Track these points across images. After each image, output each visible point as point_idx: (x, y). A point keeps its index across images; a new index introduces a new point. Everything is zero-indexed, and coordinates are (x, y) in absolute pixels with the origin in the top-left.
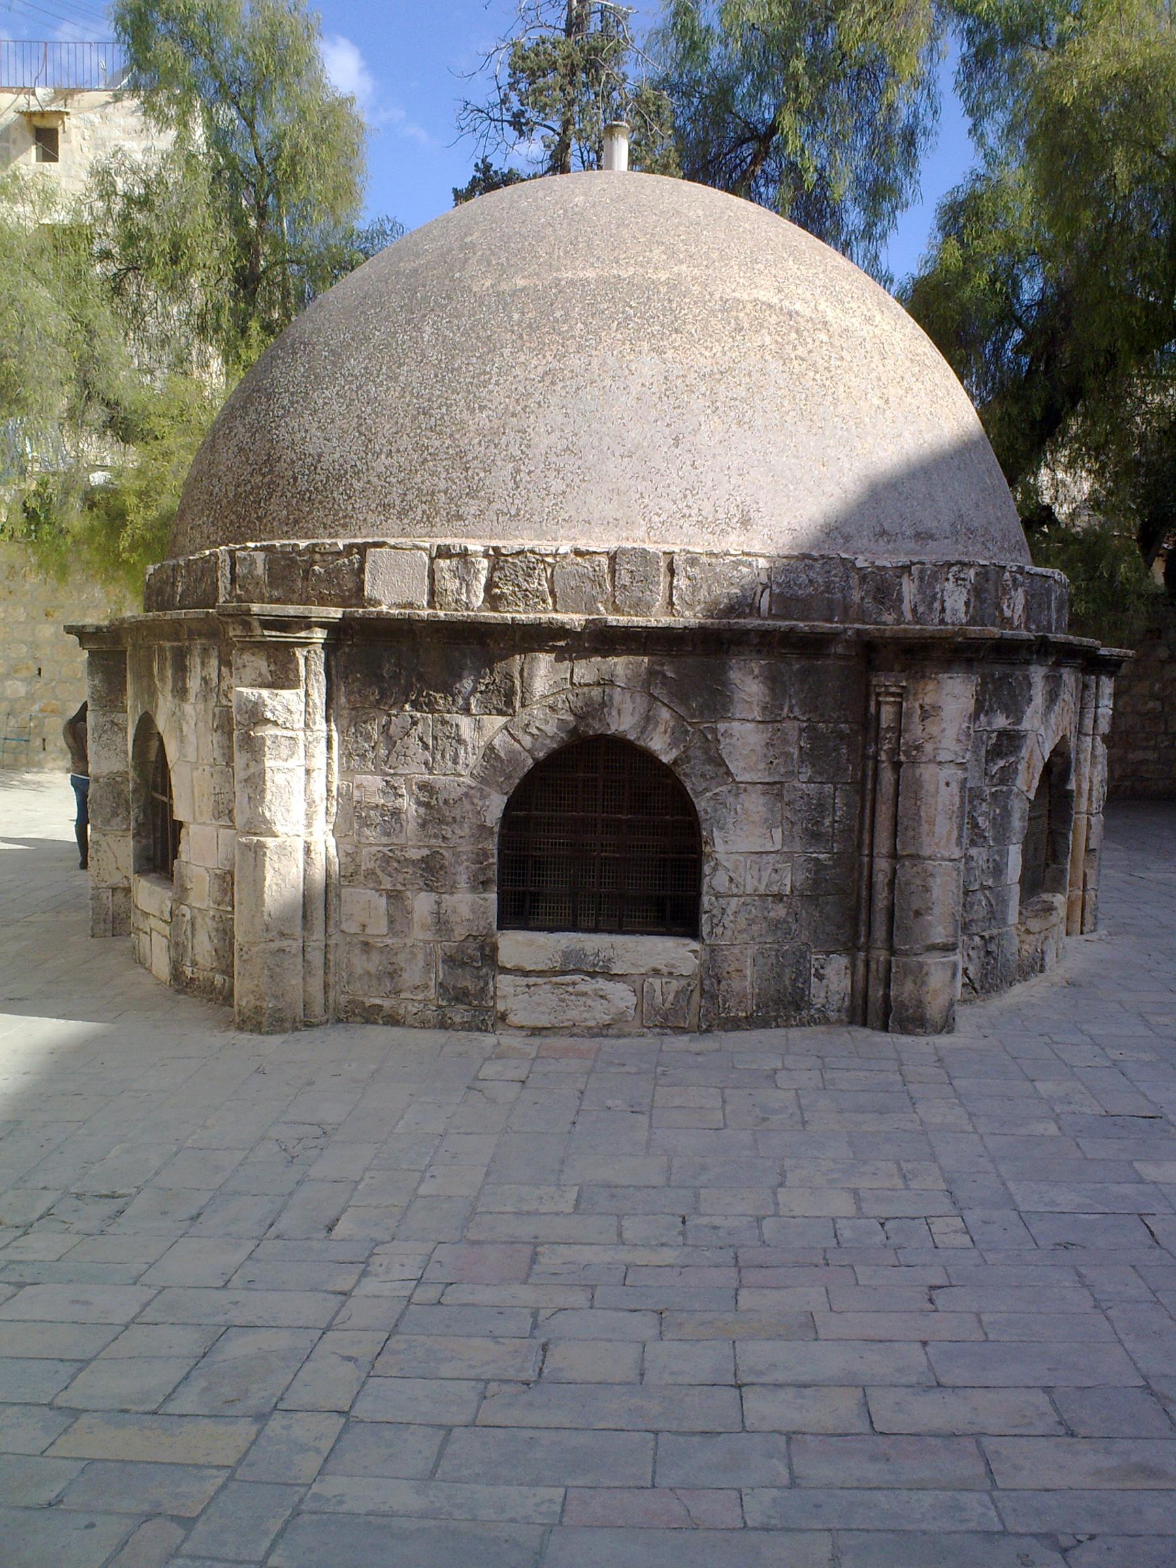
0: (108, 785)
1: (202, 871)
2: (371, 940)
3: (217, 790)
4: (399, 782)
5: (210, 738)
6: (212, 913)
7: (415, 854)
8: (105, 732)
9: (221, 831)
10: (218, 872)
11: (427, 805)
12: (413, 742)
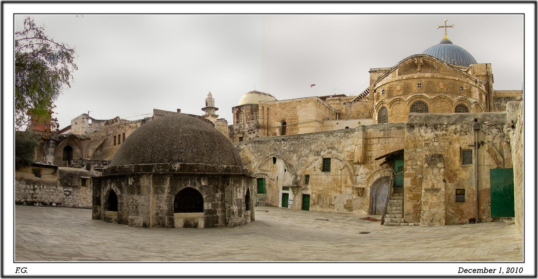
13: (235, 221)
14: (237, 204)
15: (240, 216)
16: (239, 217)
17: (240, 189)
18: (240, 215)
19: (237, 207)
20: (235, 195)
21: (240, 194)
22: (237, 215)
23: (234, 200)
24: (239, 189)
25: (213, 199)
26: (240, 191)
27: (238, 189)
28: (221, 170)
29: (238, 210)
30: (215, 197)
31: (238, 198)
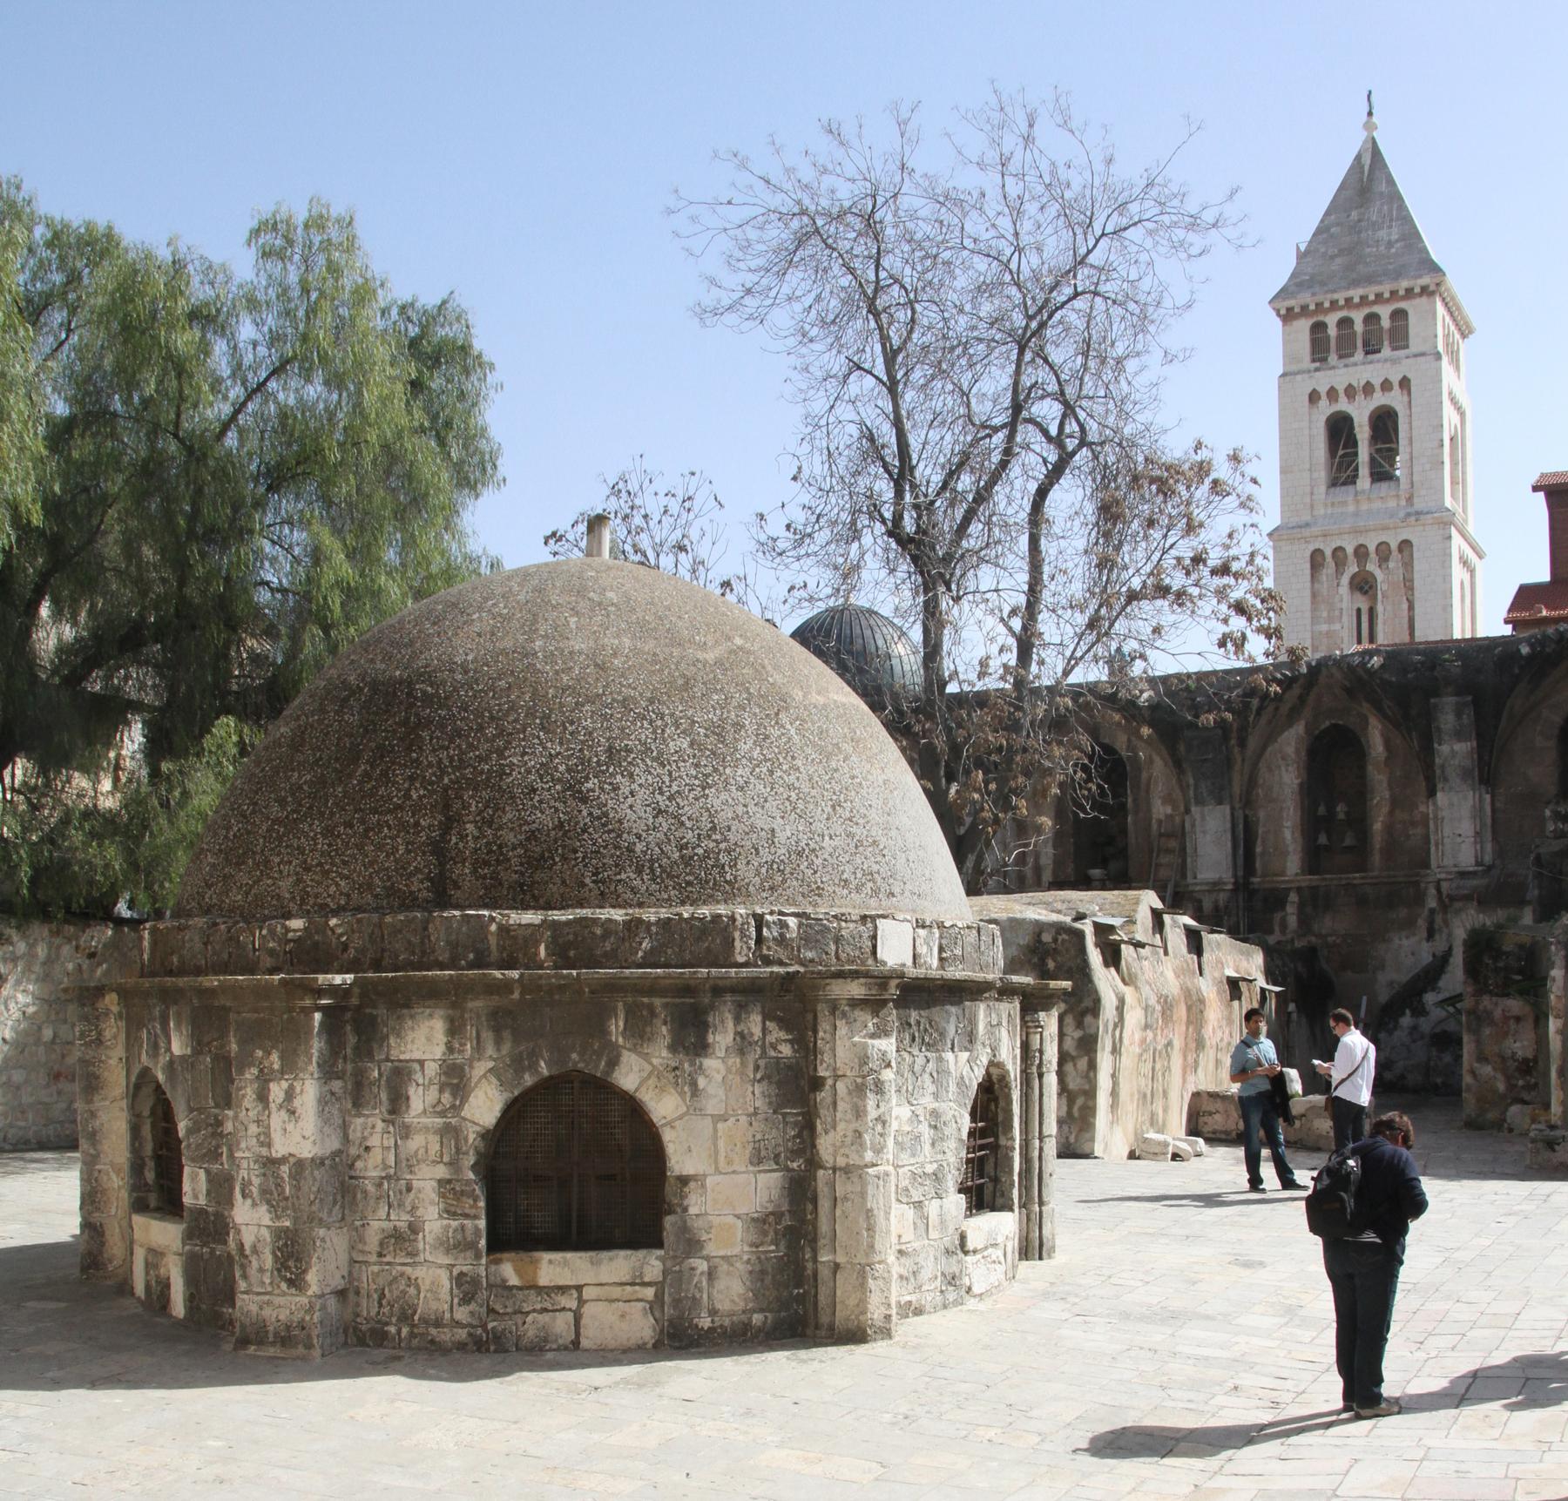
0: (331, 1167)
1: (731, 1219)
2: (903, 1247)
3: (759, 1137)
4: (920, 1111)
5: (751, 1089)
6: (745, 1257)
7: (930, 1169)
8: (326, 1103)
9: (761, 1177)
10: (756, 1215)
11: (935, 1127)
12: (926, 1076)
13: (254, 1308)
14: (264, 1192)
15: (291, 1283)
16: (284, 1286)
17: (291, 1087)
18: (287, 1268)
19: (263, 1215)
20: (253, 1129)
21: (290, 1127)
22: (269, 1261)
23: (244, 1164)
24: (285, 1085)
25: (214, 1143)
26: (297, 1103)
27: (274, 1087)
28: (272, 952)
29: (278, 1233)
30: (221, 1135)
31: (279, 1150)
